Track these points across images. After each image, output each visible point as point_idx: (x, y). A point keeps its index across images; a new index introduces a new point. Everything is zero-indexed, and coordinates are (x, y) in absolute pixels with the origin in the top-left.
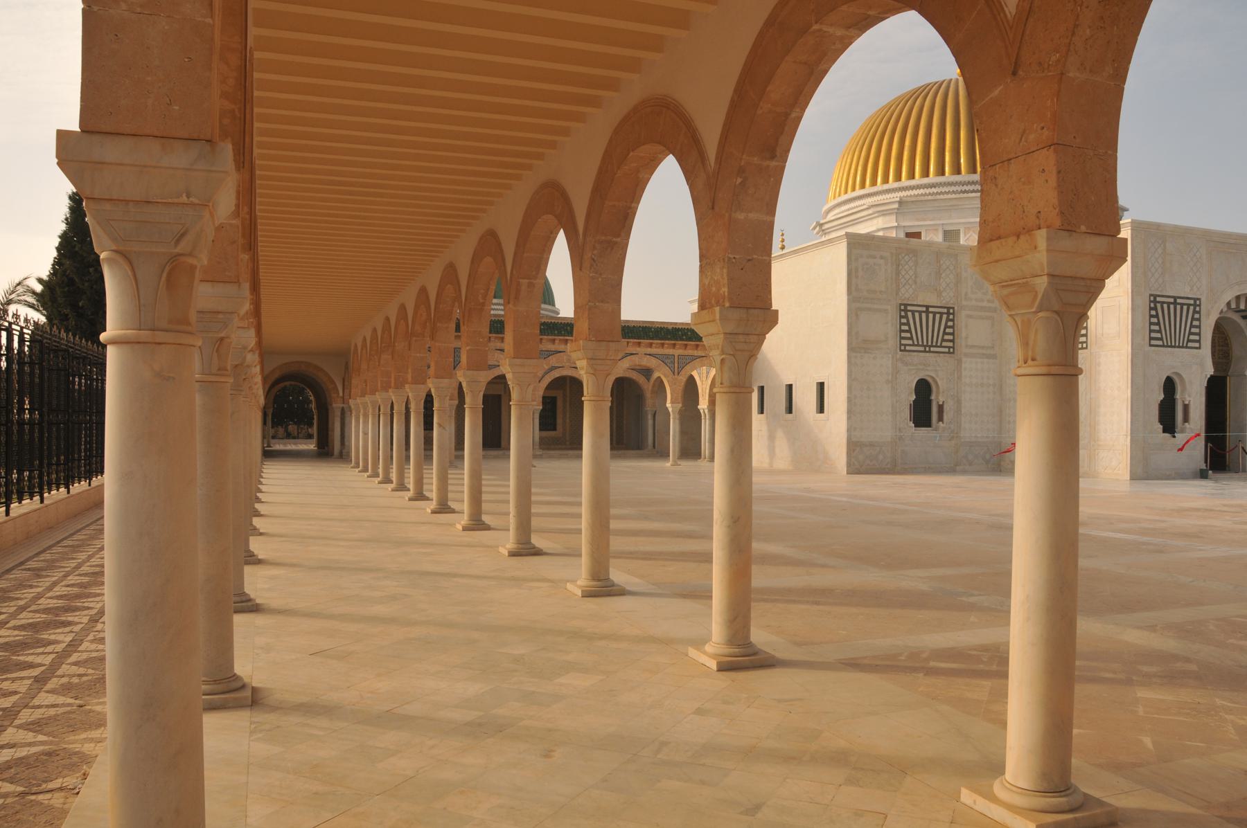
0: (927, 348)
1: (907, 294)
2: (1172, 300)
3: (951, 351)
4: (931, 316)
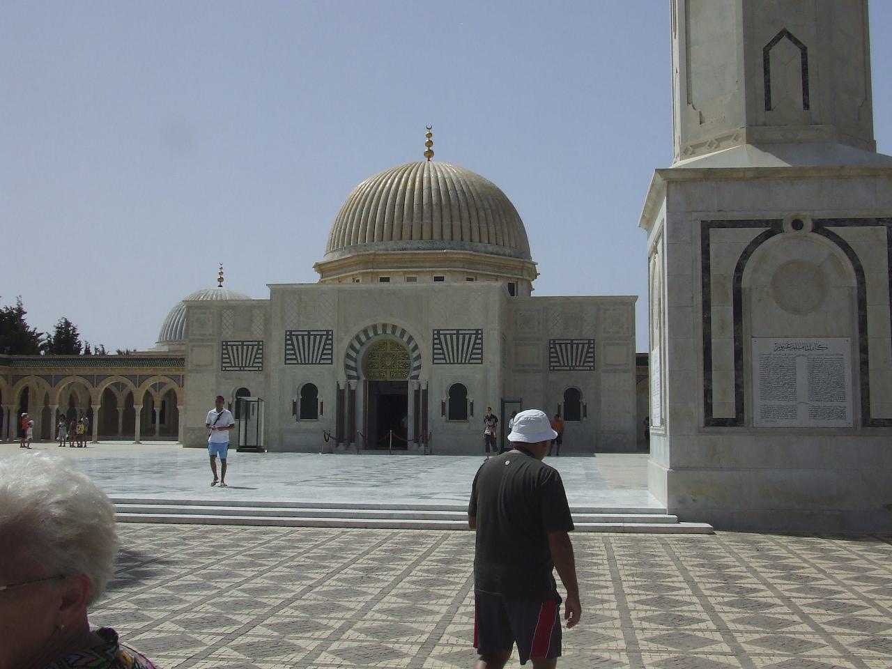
0: (241, 368)
1: (228, 334)
2: (306, 333)
3: (260, 369)
4: (245, 347)
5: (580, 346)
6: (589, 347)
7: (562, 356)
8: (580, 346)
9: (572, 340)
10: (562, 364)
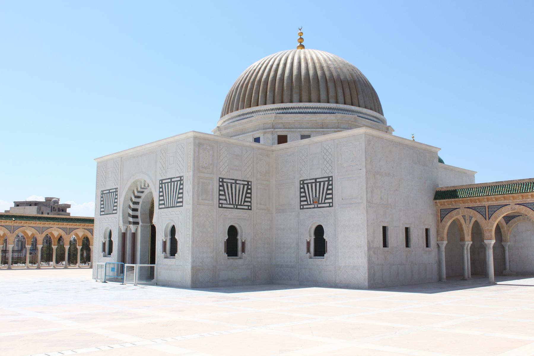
5: (322, 183)
6: (329, 185)
7: (309, 195)
8: (322, 183)
9: (316, 179)
10: (309, 203)
